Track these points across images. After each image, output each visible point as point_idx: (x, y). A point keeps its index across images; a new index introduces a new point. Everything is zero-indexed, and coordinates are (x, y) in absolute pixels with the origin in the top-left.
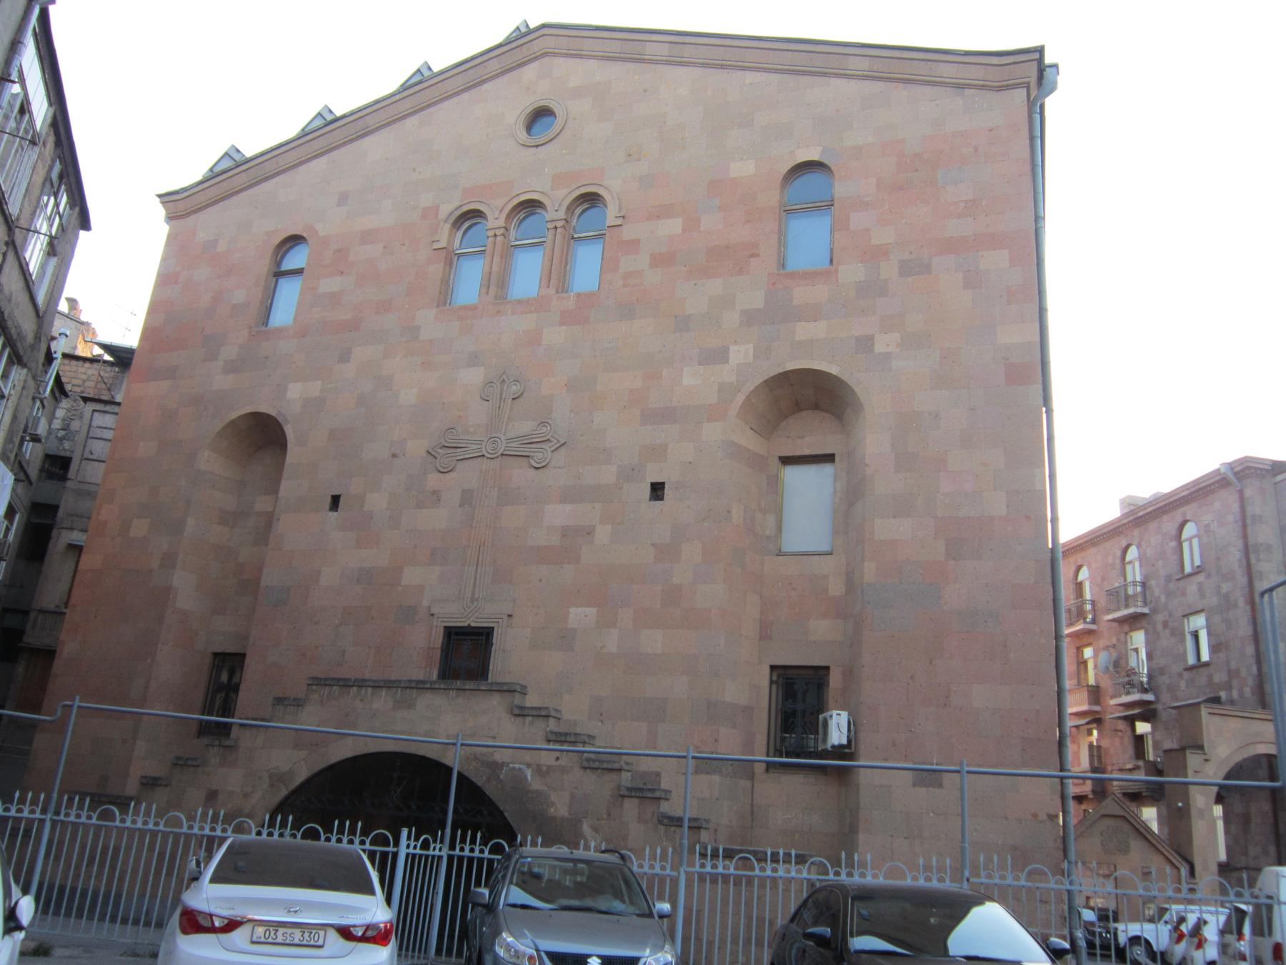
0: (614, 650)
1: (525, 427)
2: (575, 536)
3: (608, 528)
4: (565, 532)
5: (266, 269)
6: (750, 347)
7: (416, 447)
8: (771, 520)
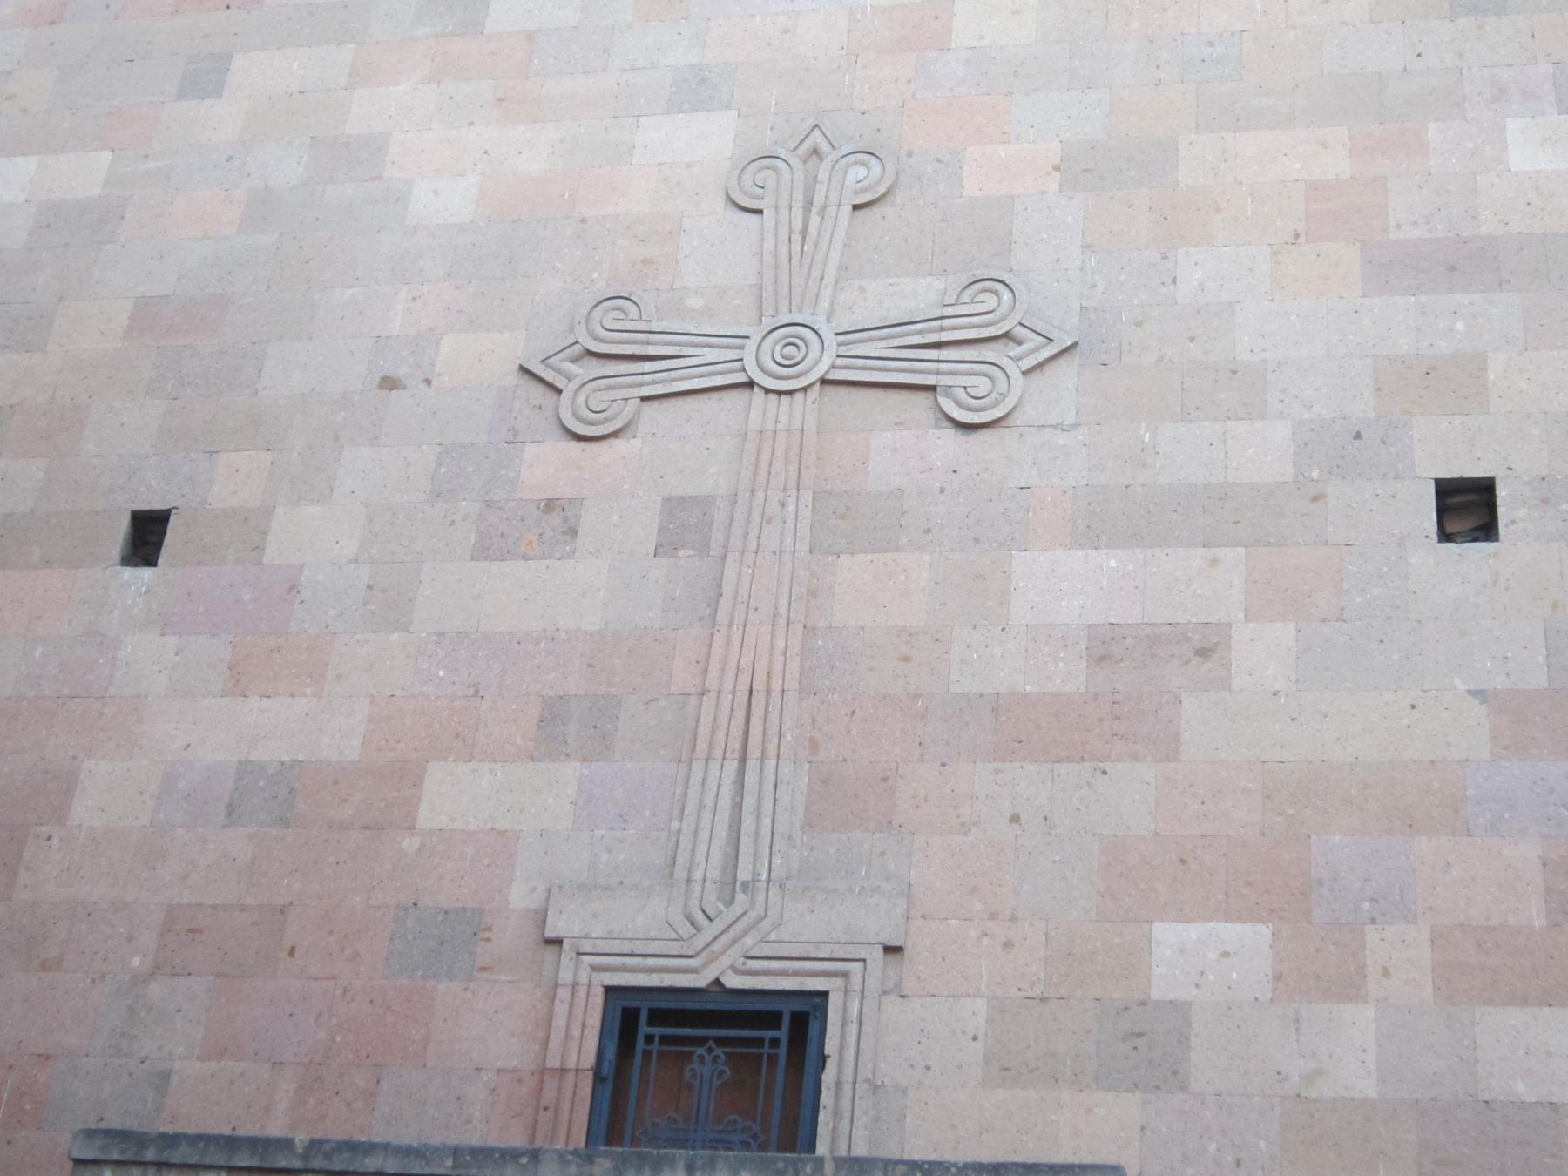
0: (1368, 1088)
1: (917, 294)
3: (1285, 632)
4: (1104, 646)
7: (477, 358)
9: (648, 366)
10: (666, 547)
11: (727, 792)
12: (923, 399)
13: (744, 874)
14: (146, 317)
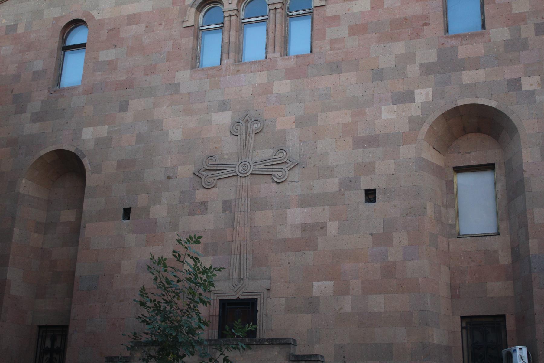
0: (349, 311)
2: (311, 232)
3: (337, 223)
4: (304, 228)
5: (57, 45)
6: (430, 90)
7: (185, 171)
8: (452, 212)
9: (218, 172)
10: (224, 211)
11: (238, 261)
12: (269, 177)
13: (242, 277)
14: (120, 164)
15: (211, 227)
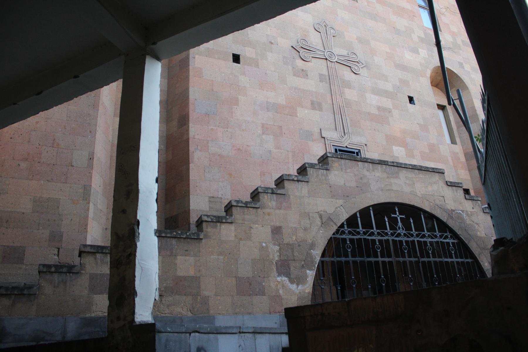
1: (345, 53)
4: (379, 108)
12: (349, 68)
15: (314, 90)
